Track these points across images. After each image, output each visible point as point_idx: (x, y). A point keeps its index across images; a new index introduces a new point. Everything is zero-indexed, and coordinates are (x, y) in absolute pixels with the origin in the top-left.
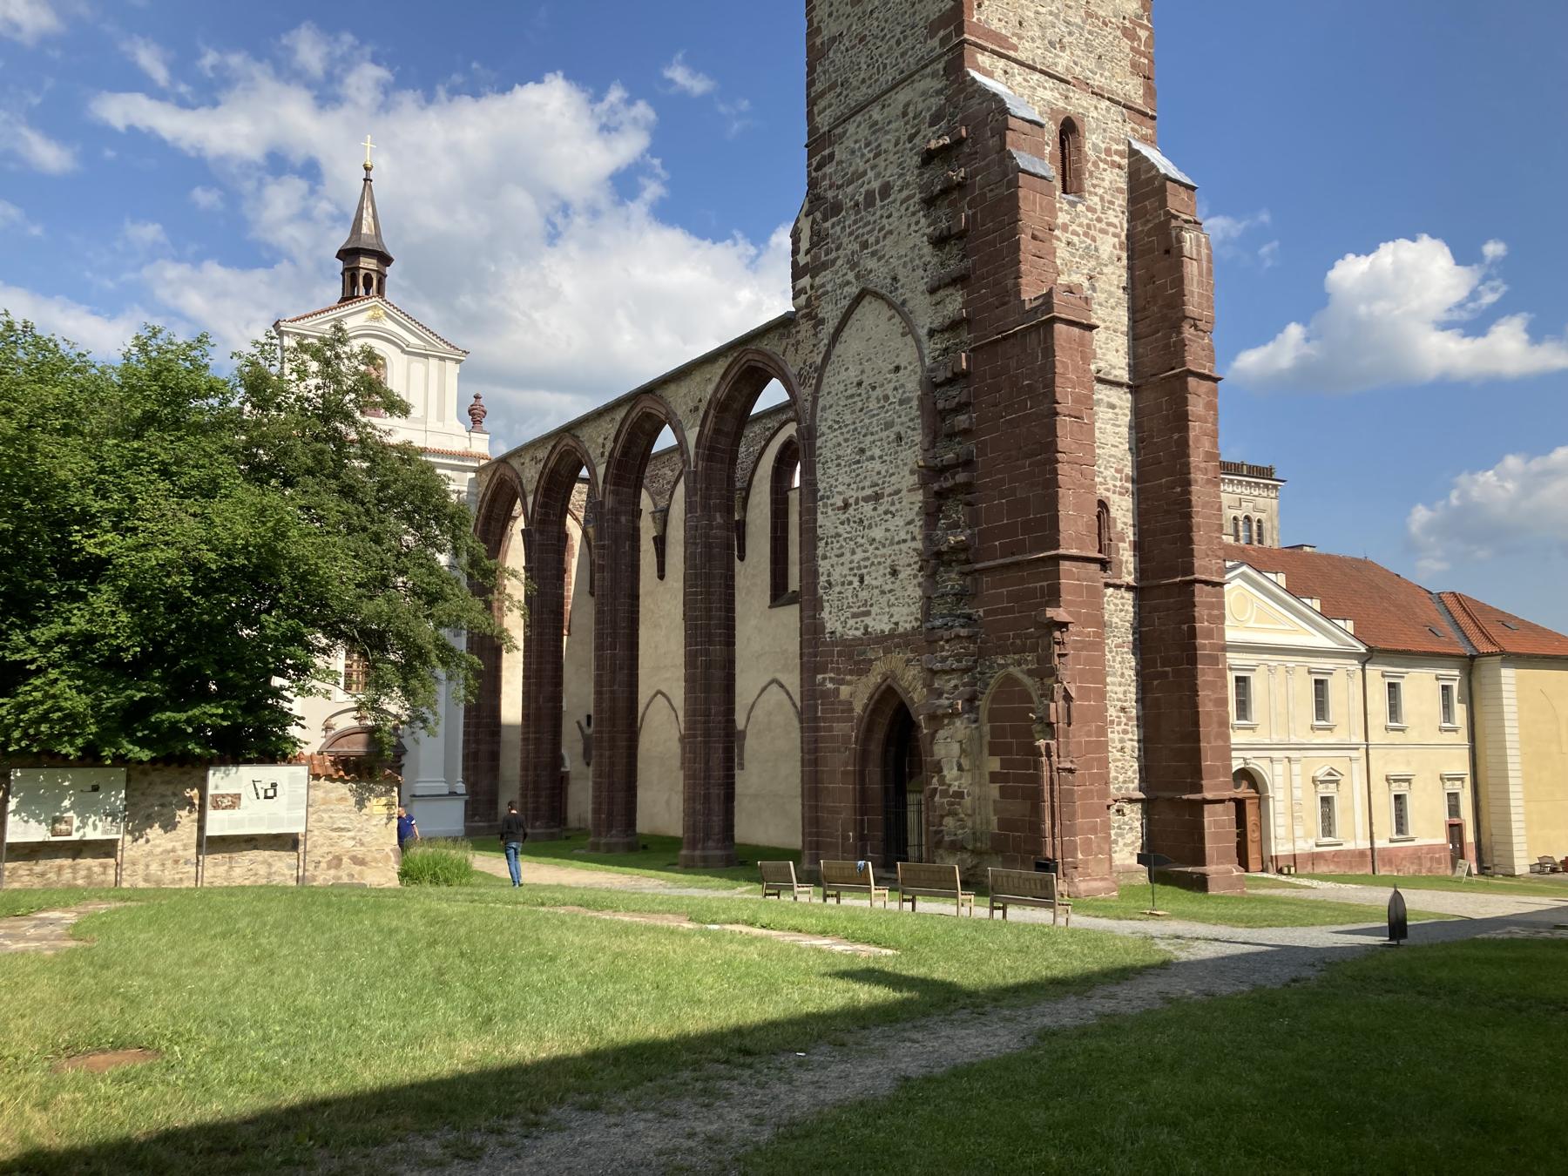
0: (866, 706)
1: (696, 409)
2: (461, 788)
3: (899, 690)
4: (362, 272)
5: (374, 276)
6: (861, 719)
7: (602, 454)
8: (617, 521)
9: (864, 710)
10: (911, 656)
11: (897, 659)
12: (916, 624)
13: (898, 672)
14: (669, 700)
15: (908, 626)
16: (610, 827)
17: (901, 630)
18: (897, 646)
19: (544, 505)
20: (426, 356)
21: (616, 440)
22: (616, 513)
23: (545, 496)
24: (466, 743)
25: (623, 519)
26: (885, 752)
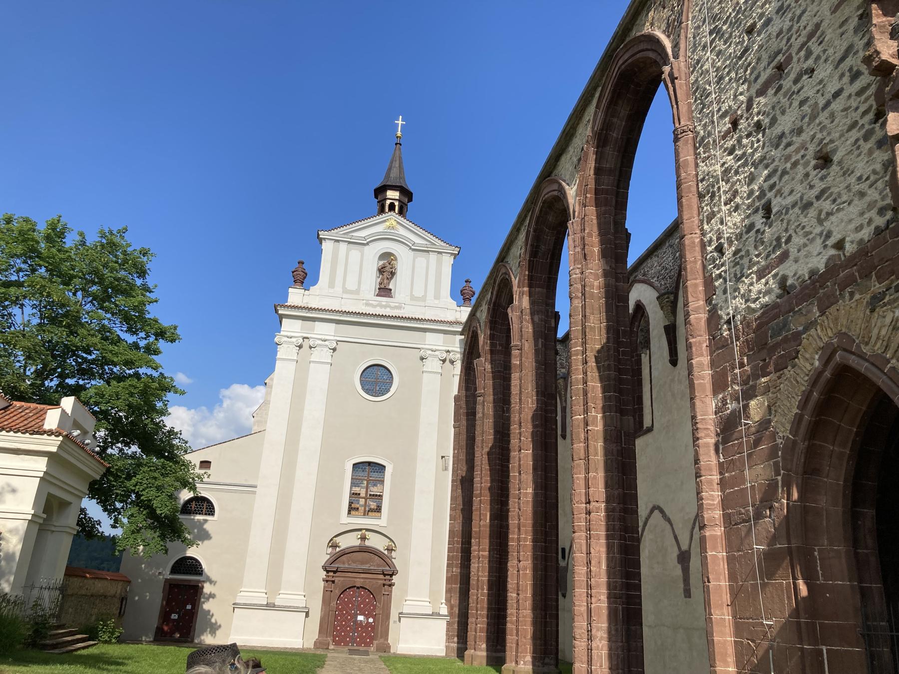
0: (798, 419)
2: (444, 610)
3: (863, 367)
4: (388, 202)
5: (397, 203)
6: (790, 446)
9: (795, 430)
10: (876, 287)
11: (850, 312)
12: (880, 221)
13: (855, 332)
15: (866, 234)
17: (850, 248)
18: (850, 281)
20: (428, 251)
21: (526, 245)
26: (853, 517)
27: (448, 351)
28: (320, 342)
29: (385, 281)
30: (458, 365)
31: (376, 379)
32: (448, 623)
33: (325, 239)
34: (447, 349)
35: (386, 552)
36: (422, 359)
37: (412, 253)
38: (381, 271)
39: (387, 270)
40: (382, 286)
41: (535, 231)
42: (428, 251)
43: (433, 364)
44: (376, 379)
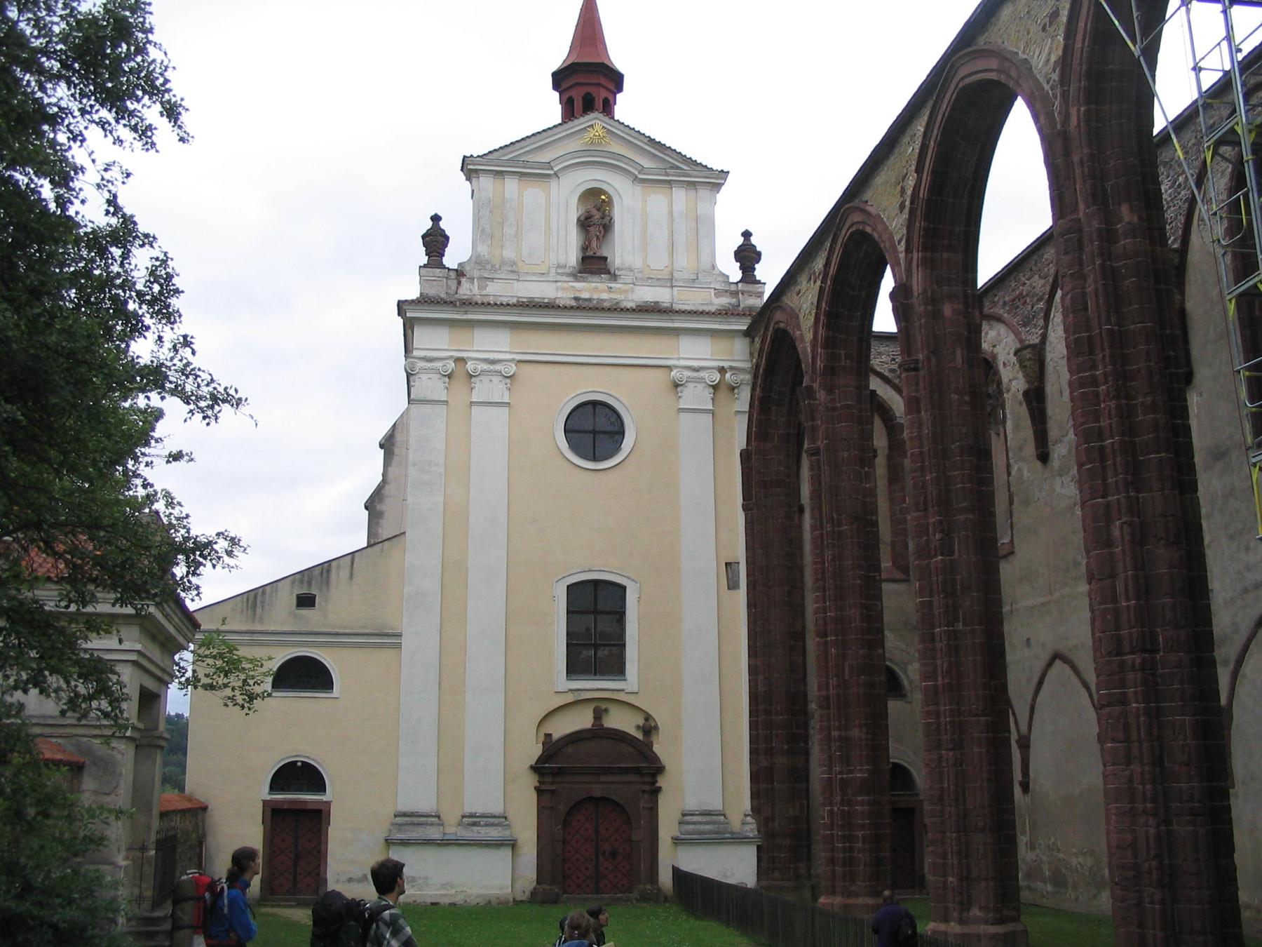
1: (1055, 15)
7: (902, 207)
8: (936, 315)
14: (1074, 668)
16: (965, 905)
19: (830, 343)
21: (919, 170)
22: (933, 300)
23: (829, 326)
24: (754, 752)
25: (947, 310)
27: (722, 370)
28: (486, 366)
29: (594, 243)
30: (745, 395)
31: (595, 430)
32: (759, 848)
33: (476, 171)
34: (721, 364)
35: (640, 736)
36: (676, 386)
37: (638, 189)
38: (585, 224)
39: (596, 219)
40: (590, 253)
41: (940, 145)
42: (669, 182)
43: (697, 396)
44: (595, 430)
